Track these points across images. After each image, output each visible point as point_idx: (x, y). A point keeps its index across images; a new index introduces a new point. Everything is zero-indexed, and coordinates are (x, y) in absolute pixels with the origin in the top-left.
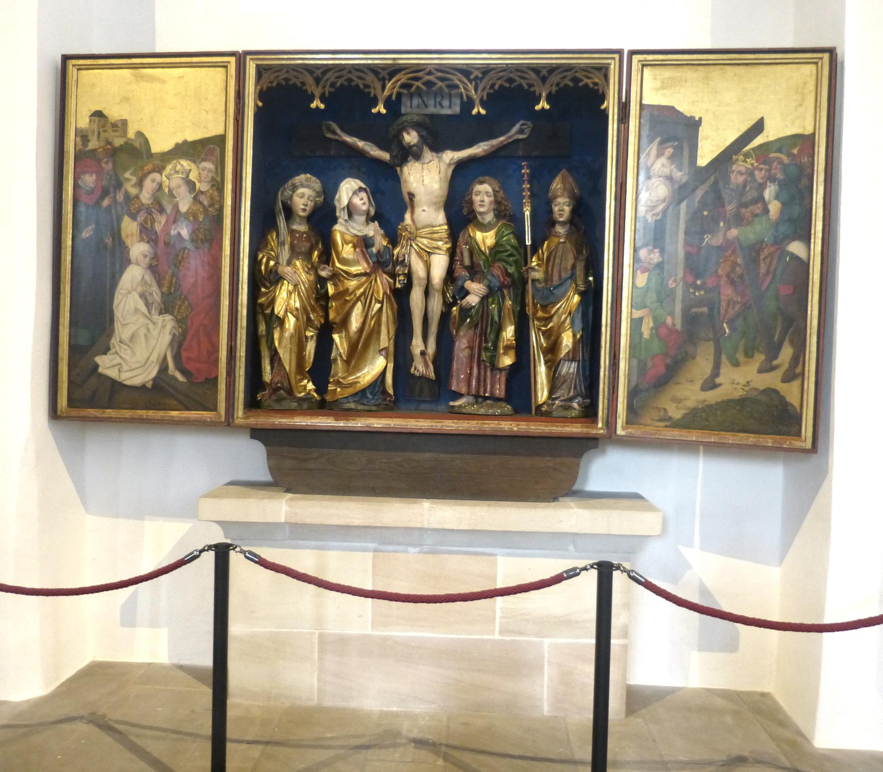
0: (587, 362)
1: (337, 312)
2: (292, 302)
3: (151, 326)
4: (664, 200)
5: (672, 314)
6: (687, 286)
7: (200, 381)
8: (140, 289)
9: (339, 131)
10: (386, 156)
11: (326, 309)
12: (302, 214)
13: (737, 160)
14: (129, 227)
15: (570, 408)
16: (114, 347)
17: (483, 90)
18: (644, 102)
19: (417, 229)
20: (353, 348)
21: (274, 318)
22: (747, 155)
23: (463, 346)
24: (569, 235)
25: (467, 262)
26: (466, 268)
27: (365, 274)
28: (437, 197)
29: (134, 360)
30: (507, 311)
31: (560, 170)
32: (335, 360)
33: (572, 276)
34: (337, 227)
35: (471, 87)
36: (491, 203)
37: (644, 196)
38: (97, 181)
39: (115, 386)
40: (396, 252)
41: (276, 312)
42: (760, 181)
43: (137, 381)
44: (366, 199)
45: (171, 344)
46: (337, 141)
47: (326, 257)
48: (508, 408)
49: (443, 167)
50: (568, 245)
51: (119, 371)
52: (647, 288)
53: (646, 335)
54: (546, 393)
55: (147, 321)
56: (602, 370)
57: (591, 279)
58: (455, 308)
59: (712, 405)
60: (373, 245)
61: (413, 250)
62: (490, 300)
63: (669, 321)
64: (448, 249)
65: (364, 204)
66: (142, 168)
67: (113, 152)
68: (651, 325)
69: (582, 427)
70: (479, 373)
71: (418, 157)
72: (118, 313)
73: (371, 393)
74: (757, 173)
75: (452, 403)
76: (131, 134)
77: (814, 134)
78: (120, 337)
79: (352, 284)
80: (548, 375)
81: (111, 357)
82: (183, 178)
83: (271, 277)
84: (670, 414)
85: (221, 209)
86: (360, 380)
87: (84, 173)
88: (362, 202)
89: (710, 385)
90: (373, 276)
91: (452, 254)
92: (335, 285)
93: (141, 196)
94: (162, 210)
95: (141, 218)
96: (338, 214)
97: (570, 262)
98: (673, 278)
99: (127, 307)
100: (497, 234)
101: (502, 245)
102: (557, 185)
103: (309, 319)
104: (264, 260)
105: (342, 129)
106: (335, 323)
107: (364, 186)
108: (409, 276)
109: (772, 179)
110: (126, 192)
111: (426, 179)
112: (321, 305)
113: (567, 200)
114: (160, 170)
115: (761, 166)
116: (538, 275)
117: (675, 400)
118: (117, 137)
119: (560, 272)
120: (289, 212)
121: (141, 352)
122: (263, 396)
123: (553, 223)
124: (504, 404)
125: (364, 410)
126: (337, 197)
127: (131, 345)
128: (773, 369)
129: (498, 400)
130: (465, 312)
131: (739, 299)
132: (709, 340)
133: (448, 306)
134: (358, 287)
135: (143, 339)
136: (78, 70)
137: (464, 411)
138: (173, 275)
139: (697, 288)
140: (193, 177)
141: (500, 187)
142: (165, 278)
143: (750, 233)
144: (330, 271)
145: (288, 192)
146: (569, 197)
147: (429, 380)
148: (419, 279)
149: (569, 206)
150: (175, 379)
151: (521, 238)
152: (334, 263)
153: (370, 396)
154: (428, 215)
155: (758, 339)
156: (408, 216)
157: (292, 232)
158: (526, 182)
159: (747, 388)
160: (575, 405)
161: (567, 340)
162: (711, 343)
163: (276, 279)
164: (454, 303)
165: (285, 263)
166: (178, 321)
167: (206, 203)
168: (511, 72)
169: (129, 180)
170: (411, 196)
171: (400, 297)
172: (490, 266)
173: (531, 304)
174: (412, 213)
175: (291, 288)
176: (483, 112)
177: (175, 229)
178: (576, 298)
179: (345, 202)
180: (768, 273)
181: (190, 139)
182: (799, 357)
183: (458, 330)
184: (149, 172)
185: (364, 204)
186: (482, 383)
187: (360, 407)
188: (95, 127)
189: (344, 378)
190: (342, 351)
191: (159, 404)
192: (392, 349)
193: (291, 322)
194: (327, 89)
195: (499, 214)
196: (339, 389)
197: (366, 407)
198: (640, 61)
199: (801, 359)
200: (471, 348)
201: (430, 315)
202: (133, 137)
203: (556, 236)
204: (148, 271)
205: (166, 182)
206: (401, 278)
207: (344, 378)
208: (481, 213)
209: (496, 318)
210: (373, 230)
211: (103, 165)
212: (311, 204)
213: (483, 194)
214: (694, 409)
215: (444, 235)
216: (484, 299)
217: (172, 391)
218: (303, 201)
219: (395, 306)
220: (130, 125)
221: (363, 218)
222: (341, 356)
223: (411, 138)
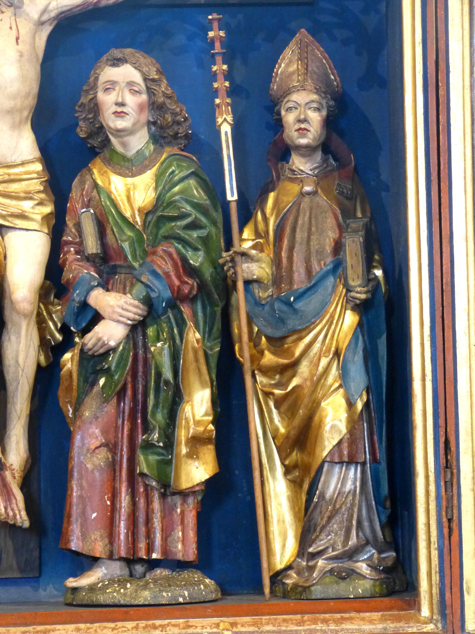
0: (383, 466)
23: (94, 443)
24: (322, 176)
25: (92, 245)
26: (89, 259)
28: (14, 97)
30: (191, 355)
36: (141, 108)
48: (207, 586)
49: (25, 28)
50: (322, 200)
54: (292, 546)
57: (379, 273)
58: (67, 356)
62: (151, 331)
64: (46, 218)
69: (383, 620)
70: (134, 504)
75: (71, 582)
80: (294, 501)
91: (57, 229)
97: (331, 235)
100: (158, 178)
101: (171, 204)
102: (288, 64)
113: (315, 97)
116: (258, 268)
119: (308, 261)
123: (284, 152)
124: (197, 576)
129: (181, 565)
130: (94, 363)
137: (101, 599)
141: (158, 71)
146: (318, 91)
149: (318, 110)
158: (219, 59)
160: (363, 568)
161: (335, 417)
164: (67, 344)
172: (146, 253)
173: (245, 338)
178: (350, 319)
183: (78, 406)
186: (142, 529)
195: (161, 135)
200: (112, 447)
203: (292, 180)
208: (119, 132)
209: (168, 374)
213: (122, 90)
215: (36, 185)
216: (137, 329)
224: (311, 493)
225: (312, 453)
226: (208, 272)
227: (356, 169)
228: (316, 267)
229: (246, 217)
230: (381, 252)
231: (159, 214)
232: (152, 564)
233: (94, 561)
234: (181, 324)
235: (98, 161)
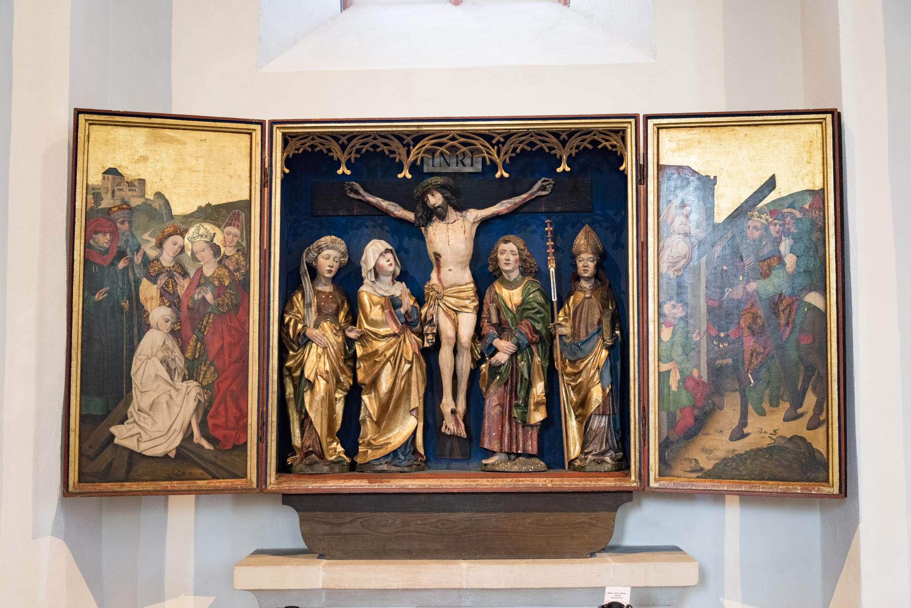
0: (618, 416)
1: (366, 372)
2: (321, 365)
3: (173, 393)
4: (685, 257)
5: (698, 366)
6: (710, 339)
8: (161, 355)
9: (361, 191)
10: (410, 216)
11: (354, 370)
12: (328, 275)
13: (752, 216)
14: (149, 291)
15: (603, 461)
16: (132, 416)
17: (506, 153)
18: (661, 163)
19: (444, 288)
20: (384, 409)
21: (303, 381)
22: (761, 212)
23: (494, 404)
24: (594, 289)
25: (494, 320)
26: (494, 325)
27: (395, 335)
29: (155, 428)
30: (536, 367)
31: (584, 225)
32: (364, 421)
33: (600, 330)
34: (363, 288)
35: (494, 151)
36: (516, 261)
37: (666, 255)
38: (111, 241)
39: (134, 456)
40: (423, 311)
41: (306, 376)
42: (774, 235)
43: (159, 451)
44: (392, 261)
45: (196, 410)
46: (360, 200)
47: (353, 318)
48: (541, 465)
49: (468, 226)
50: (594, 300)
51: (138, 441)
52: (672, 343)
53: (674, 388)
54: (578, 448)
55: (169, 388)
56: (632, 423)
57: (618, 332)
58: (484, 366)
59: (741, 455)
60: (401, 306)
61: (441, 310)
62: (519, 357)
63: (695, 373)
64: (475, 307)
65: (391, 265)
68: (678, 377)
69: (615, 481)
70: (511, 429)
71: (442, 218)
72: (136, 380)
73: (403, 454)
74: (772, 227)
75: (484, 462)
77: (823, 189)
78: (139, 406)
79: (380, 345)
80: (579, 430)
82: (206, 242)
83: (300, 340)
84: (701, 465)
85: (248, 274)
86: (391, 441)
88: (389, 264)
89: (739, 434)
90: (402, 337)
91: (479, 311)
92: (363, 346)
93: (161, 259)
94: (185, 274)
96: (364, 274)
97: (597, 316)
98: (697, 331)
100: (523, 291)
101: (528, 303)
103: (338, 381)
104: (292, 323)
105: (365, 190)
106: (365, 385)
107: (390, 247)
108: (438, 336)
109: (788, 234)
110: (145, 253)
111: (451, 239)
112: (348, 366)
113: (591, 256)
114: (182, 234)
115: (776, 221)
116: (566, 330)
117: (704, 450)
119: (587, 328)
120: (314, 273)
121: (163, 420)
122: (294, 460)
123: (578, 278)
124: (537, 460)
125: (397, 472)
126: (363, 258)
127: (151, 413)
128: (798, 417)
129: (531, 456)
130: (495, 370)
131: (762, 350)
132: (735, 390)
133: (477, 363)
134: (388, 349)
135: (165, 406)
137: (497, 469)
138: (198, 340)
139: (721, 340)
140: (218, 240)
141: (524, 245)
142: (188, 343)
143: (776, 283)
144: (358, 332)
145: (312, 255)
146: (593, 253)
147: (459, 438)
148: (449, 338)
150: (202, 447)
151: (547, 296)
152: (361, 321)
153: (402, 457)
154: (453, 274)
155: (782, 389)
156: (434, 275)
157: (318, 293)
159: (774, 437)
160: (608, 459)
161: (597, 395)
162: (738, 393)
163: (304, 341)
164: (482, 361)
165: (312, 326)
166: (203, 387)
167: (231, 268)
168: (532, 136)
170: (438, 256)
171: (430, 355)
172: (517, 324)
173: (559, 360)
174: (439, 272)
175: (320, 350)
176: (506, 175)
177: (199, 293)
178: (605, 353)
179: (372, 264)
180: (787, 324)
181: (214, 203)
182: (822, 404)
183: (488, 387)
184: (170, 235)
185: (391, 265)
186: (514, 441)
187: (394, 468)
189: (375, 440)
190: (371, 412)
191: (184, 473)
192: (421, 409)
193: (321, 386)
194: (353, 155)
195: (524, 272)
196: (370, 451)
197: (398, 469)
198: (655, 125)
199: (825, 406)
200: (502, 405)
201: (459, 374)
203: (581, 291)
205: (188, 245)
206: (430, 337)
207: (375, 440)
208: (506, 271)
209: (526, 375)
210: (399, 290)
212: (336, 266)
213: (508, 253)
214: (725, 459)
215: (471, 293)
216: (513, 356)
218: (329, 262)
219: (424, 365)
221: (390, 278)
222: (370, 417)
223: (435, 200)
224: (586, 427)
225: (587, 410)
226: (544, 332)
227: (610, 285)
228: (590, 331)
229: (561, 304)
230: (620, 322)
231: (523, 307)
232: (518, 455)
233: (493, 453)
234: (532, 354)
235: (497, 282)
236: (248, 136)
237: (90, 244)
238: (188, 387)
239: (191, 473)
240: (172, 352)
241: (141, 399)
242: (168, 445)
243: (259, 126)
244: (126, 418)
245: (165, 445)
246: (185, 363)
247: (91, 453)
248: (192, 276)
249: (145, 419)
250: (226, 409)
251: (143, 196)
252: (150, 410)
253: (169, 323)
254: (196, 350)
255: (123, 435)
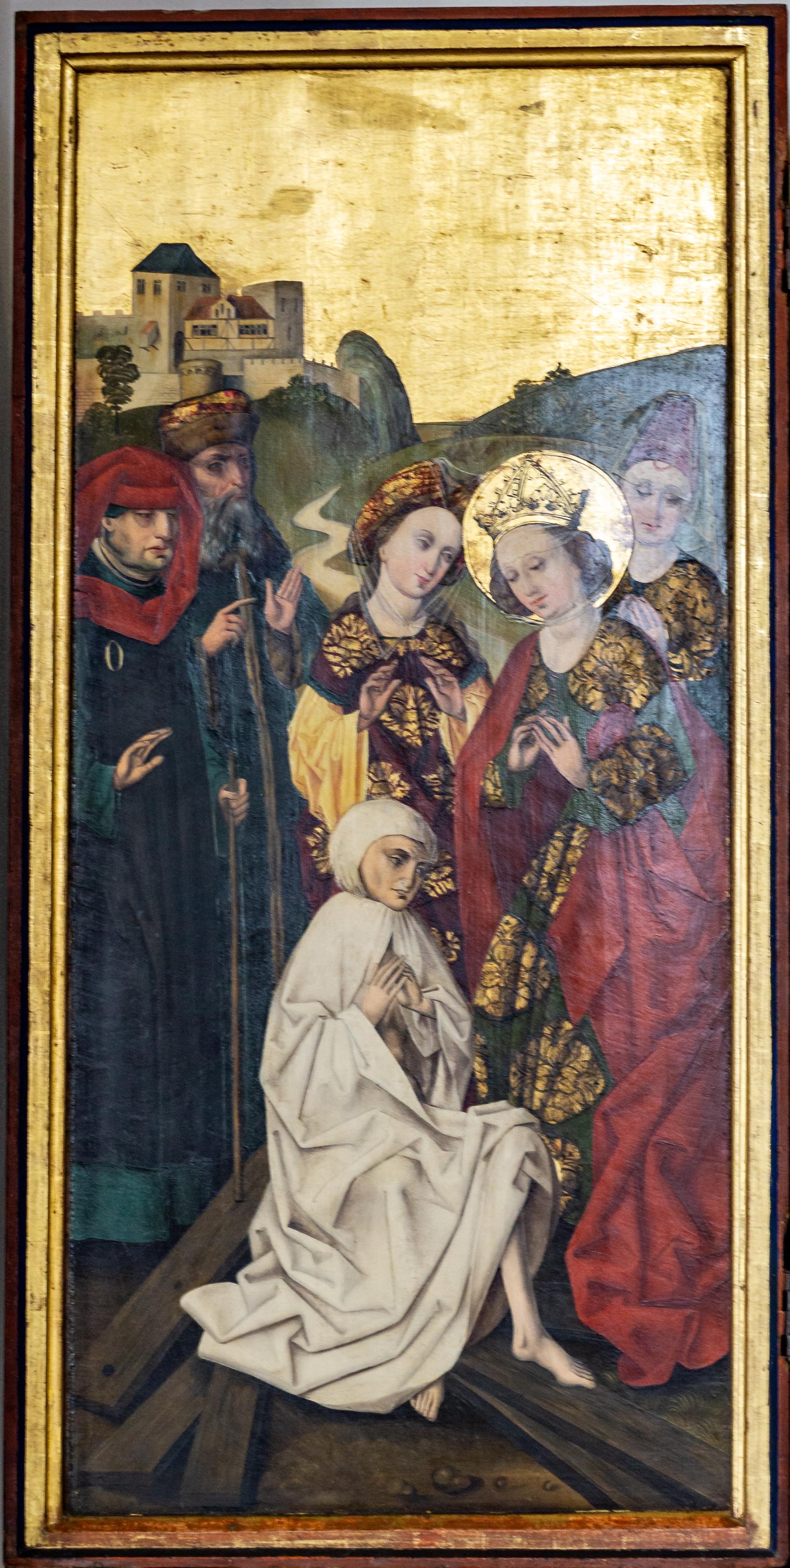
7: (649, 1381)
8: (377, 999)
14: (323, 739)
16: (268, 1247)
29: (358, 1299)
39: (277, 1415)
43: (373, 1392)
45: (522, 1225)
51: (294, 1348)
55: (412, 1133)
66: (374, 490)
67: (242, 422)
72: (281, 1102)
76: (320, 347)
78: (294, 1206)
81: (255, 1290)
82: (554, 530)
87: (115, 510)
93: (372, 607)
94: (467, 667)
95: (373, 700)
99: (321, 1074)
110: (305, 582)
114: (454, 500)
118: (262, 355)
121: (389, 1263)
127: (341, 1235)
135: (395, 1206)
136: (78, 71)
138: (521, 937)
142: (485, 946)
150: (547, 1377)
166: (546, 1129)
169: (323, 537)
177: (527, 742)
184: (406, 507)
188: (162, 314)
191: (476, 1483)
202: (330, 359)
204: (415, 925)
205: (480, 550)
211: (201, 475)
217: (525, 1427)
220: (314, 309)
236: (719, 73)
237: (91, 555)
238: (487, 1127)
239: (501, 1484)
240: (422, 987)
241: (299, 1181)
242: (411, 1367)
243: (762, 32)
244: (244, 1256)
245: (401, 1366)
246: (476, 1028)
247: (108, 1394)
248: (495, 672)
249: (317, 1258)
250: (643, 1218)
251: (294, 350)
252: (339, 1220)
253: (409, 868)
254: (516, 976)
255: (231, 1324)
